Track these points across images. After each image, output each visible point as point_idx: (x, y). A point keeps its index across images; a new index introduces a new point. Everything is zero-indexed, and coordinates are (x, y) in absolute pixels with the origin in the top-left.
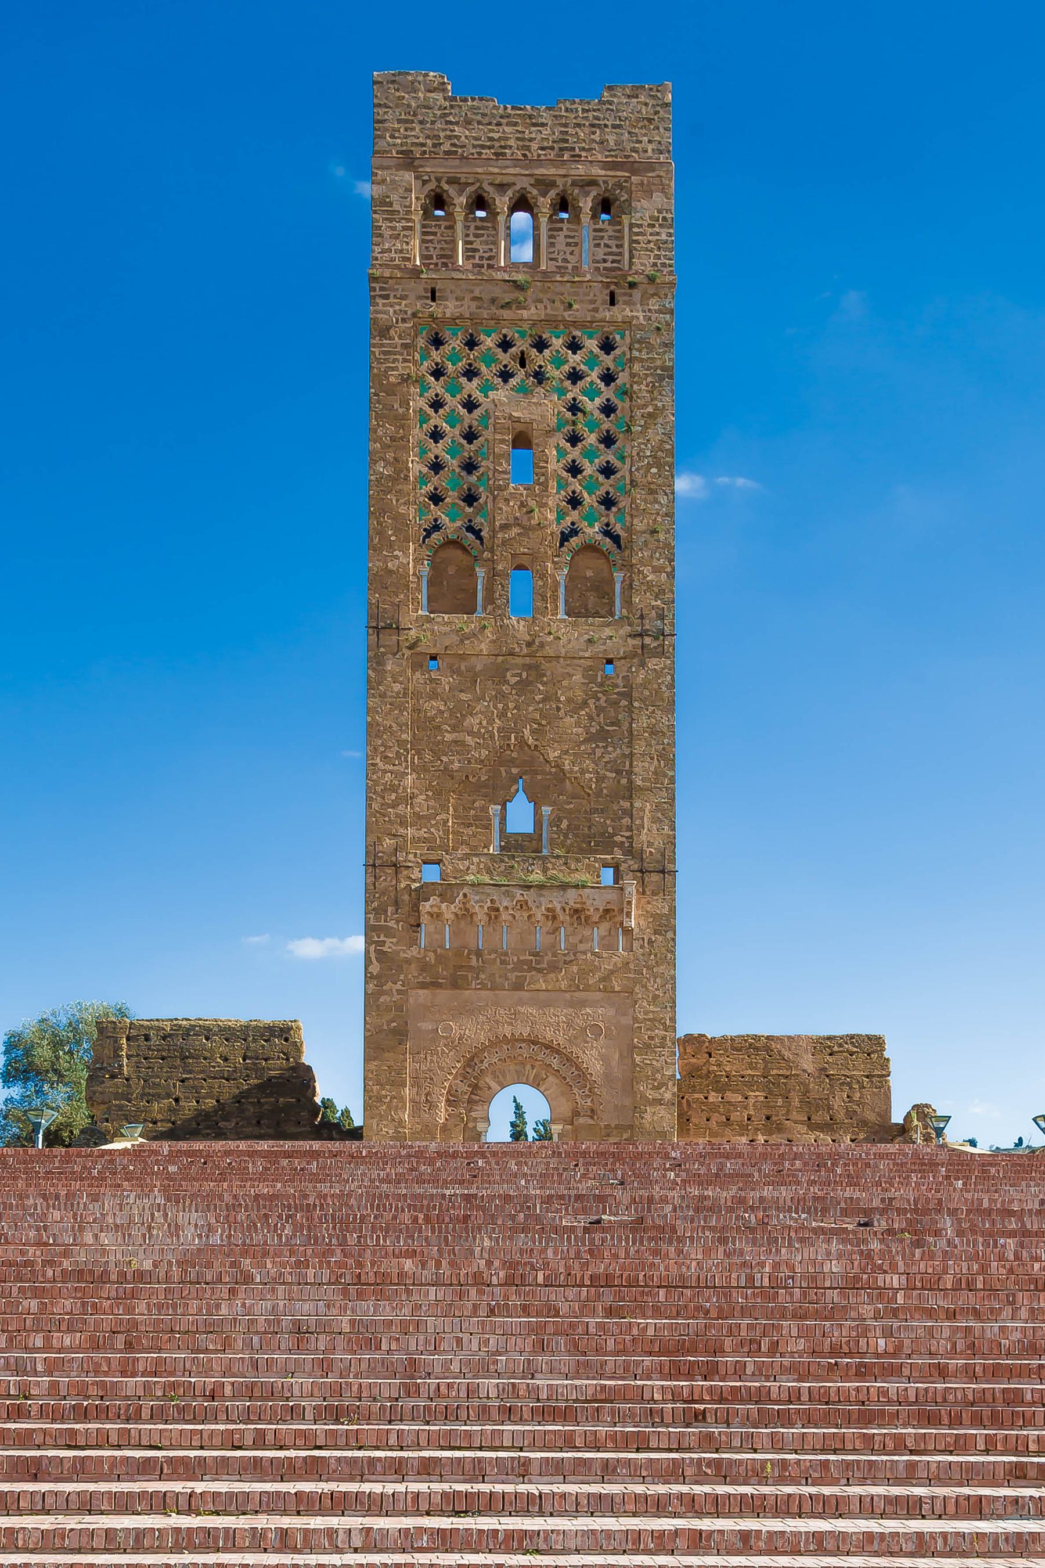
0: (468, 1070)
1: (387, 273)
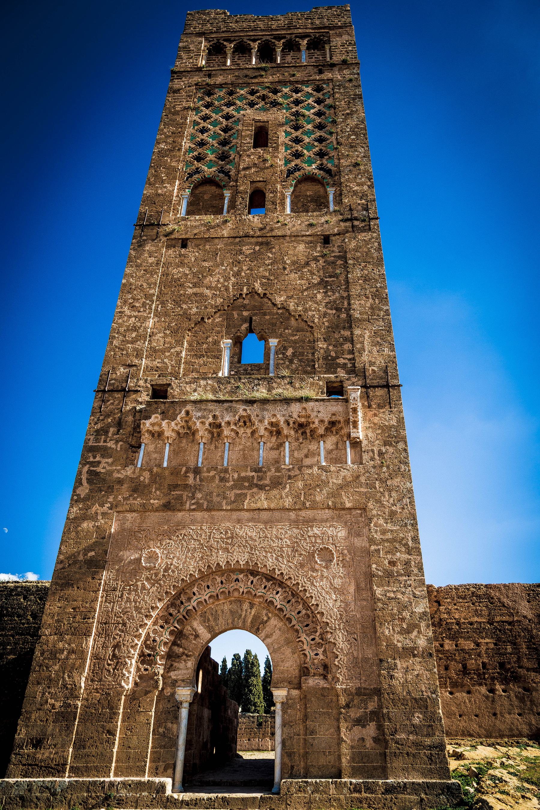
0: (171, 610)
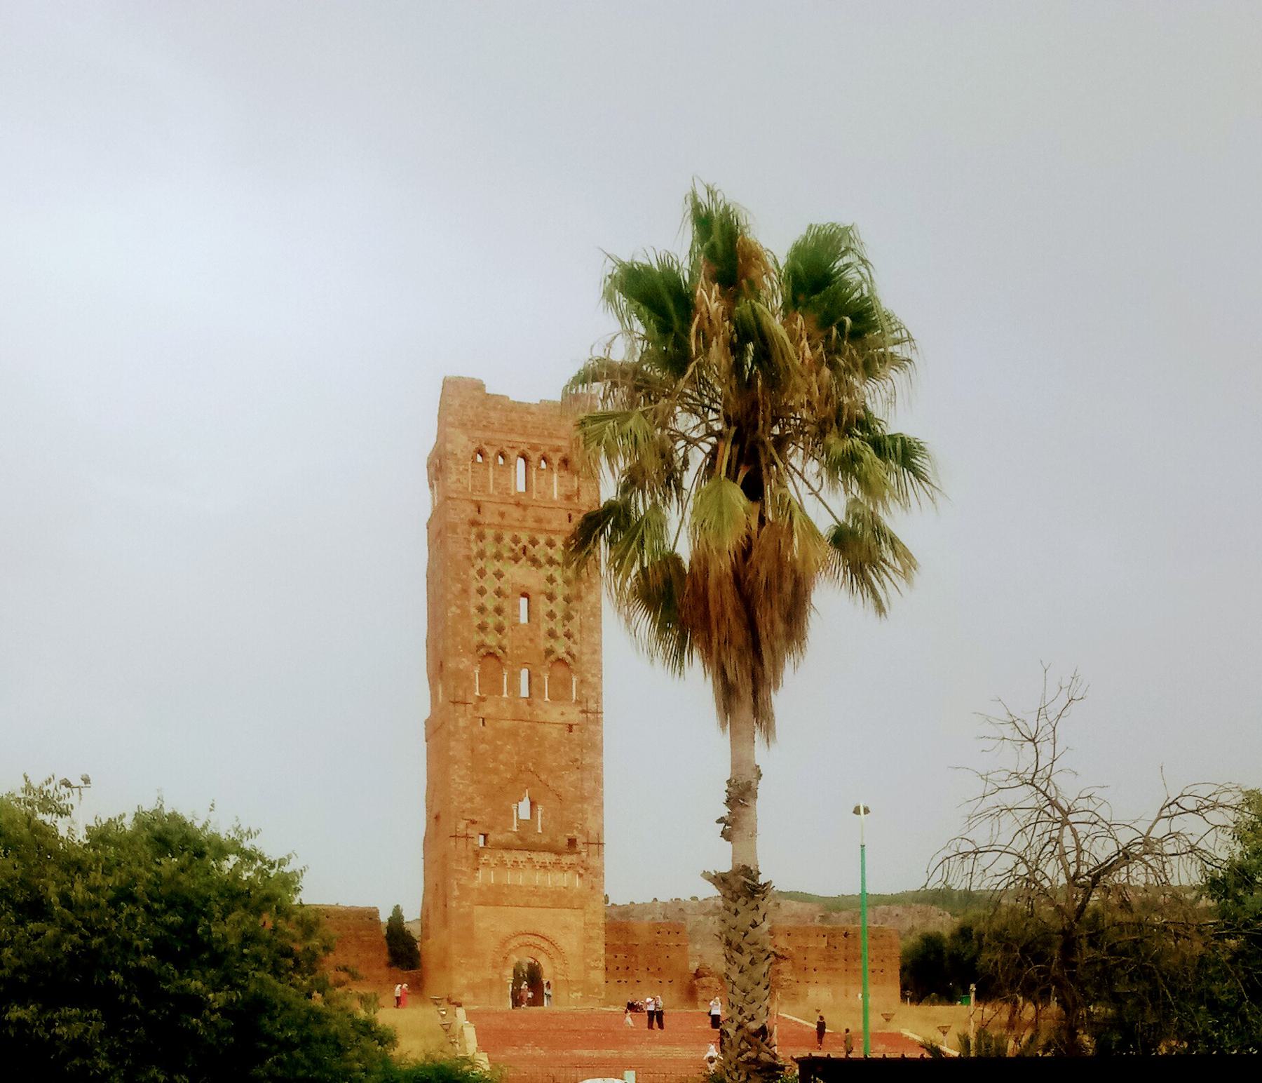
1: (455, 496)
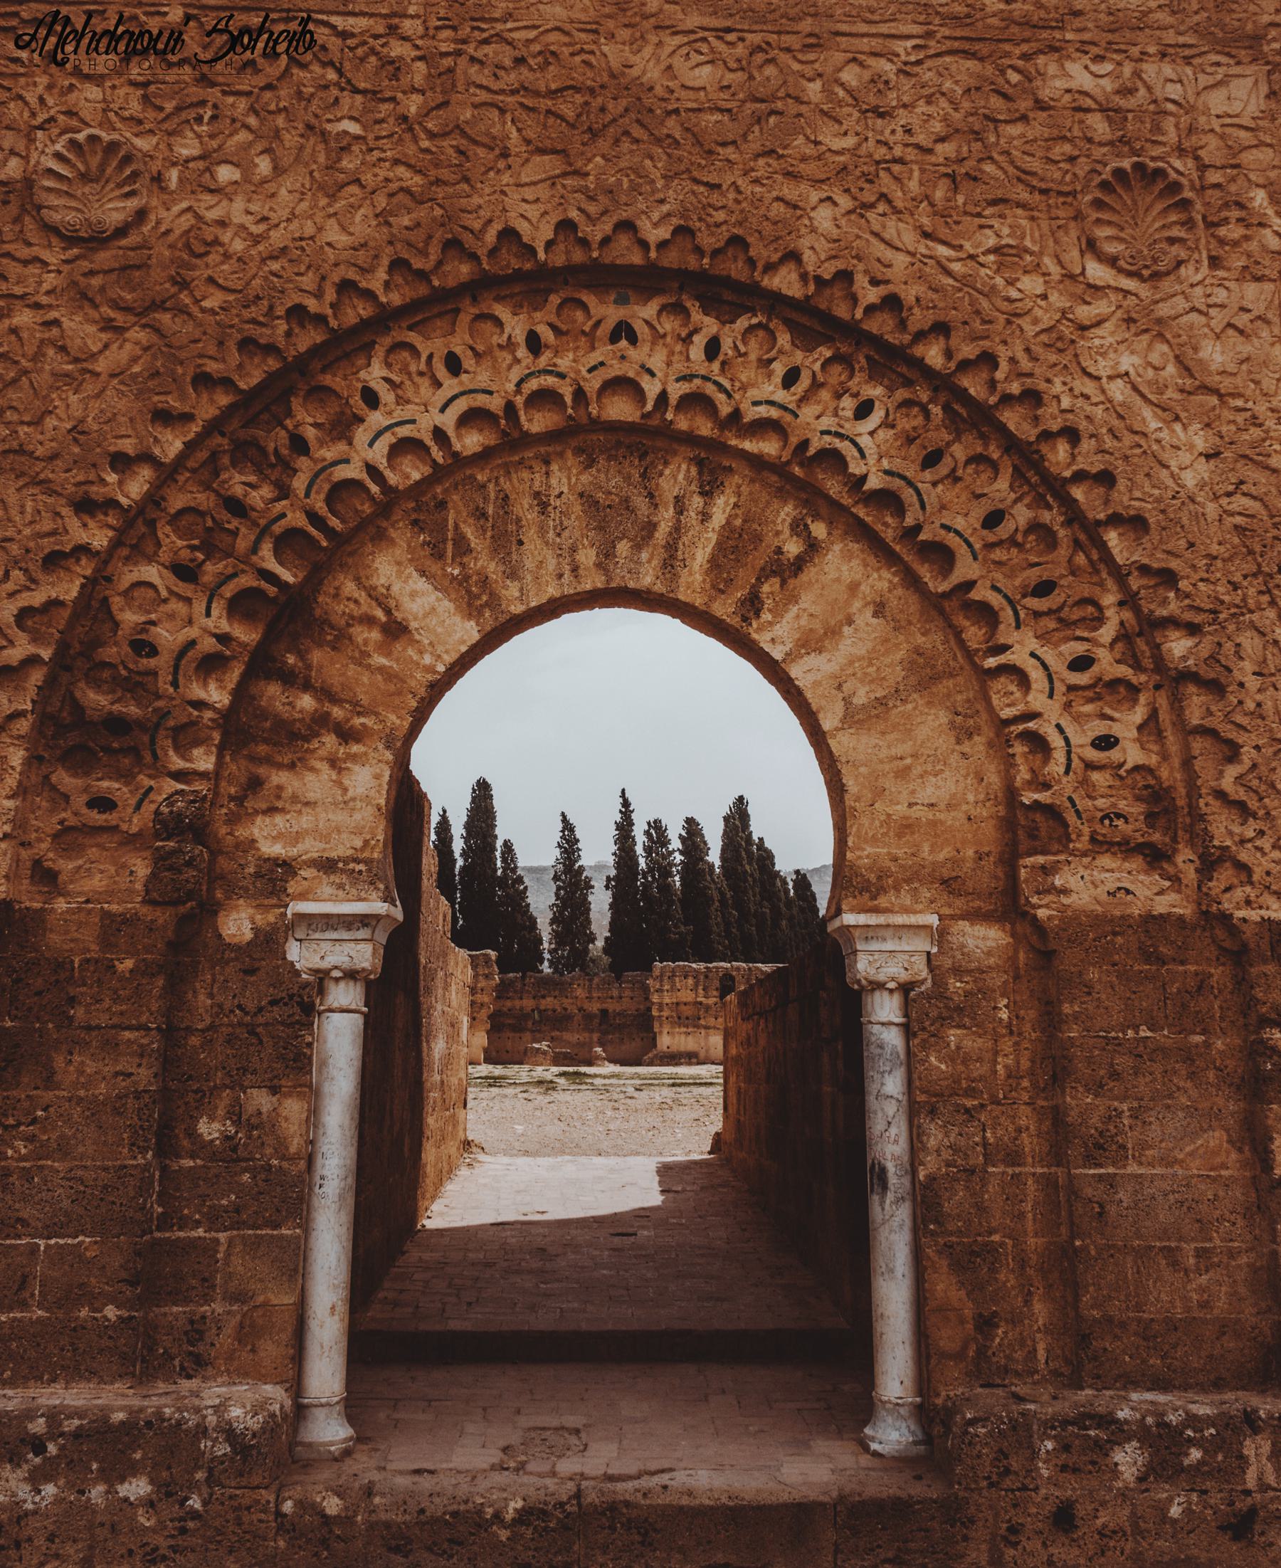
0: (237, 482)
